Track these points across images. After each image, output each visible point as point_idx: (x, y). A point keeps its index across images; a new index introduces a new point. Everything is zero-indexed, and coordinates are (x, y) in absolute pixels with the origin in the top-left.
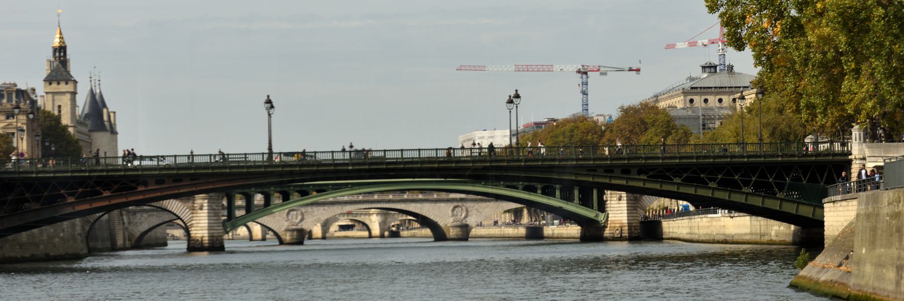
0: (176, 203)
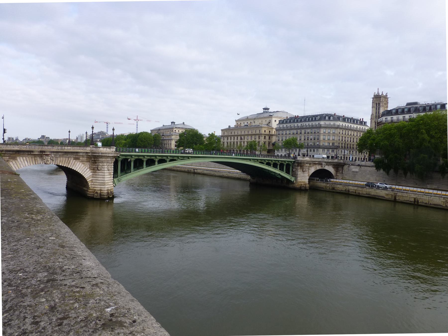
0: (79, 164)
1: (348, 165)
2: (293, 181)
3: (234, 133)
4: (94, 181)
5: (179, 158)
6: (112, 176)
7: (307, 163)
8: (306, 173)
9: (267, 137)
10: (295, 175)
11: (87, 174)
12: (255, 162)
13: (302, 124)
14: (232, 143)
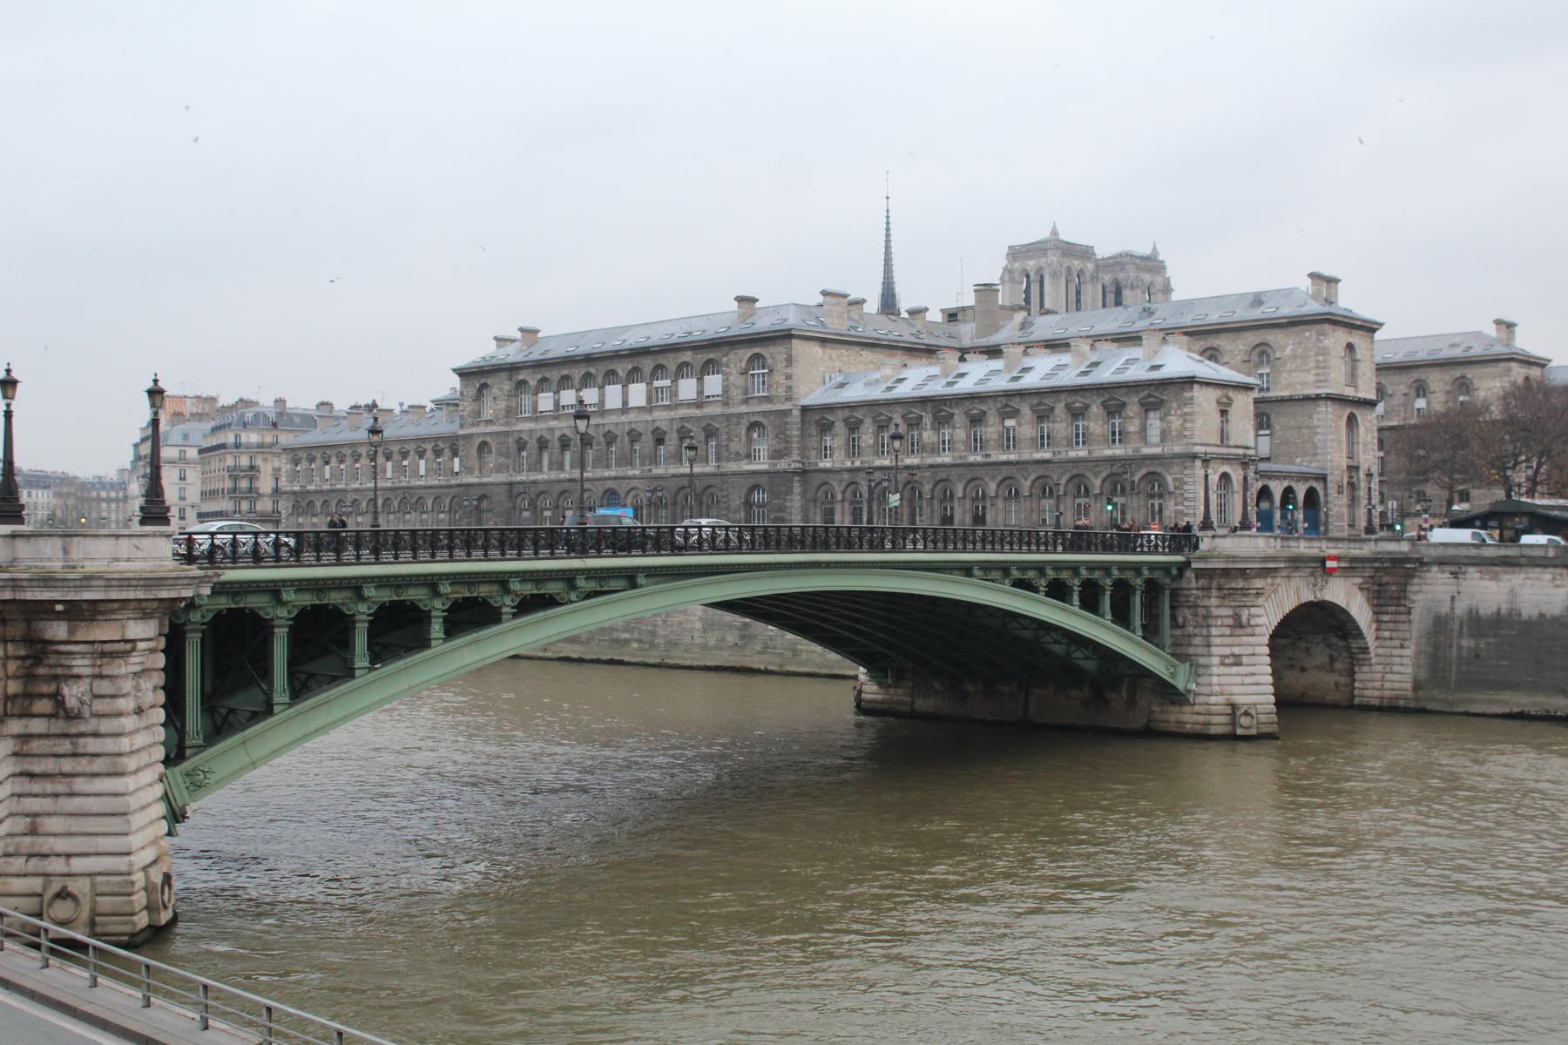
2: (1180, 686)
12: (993, 581)
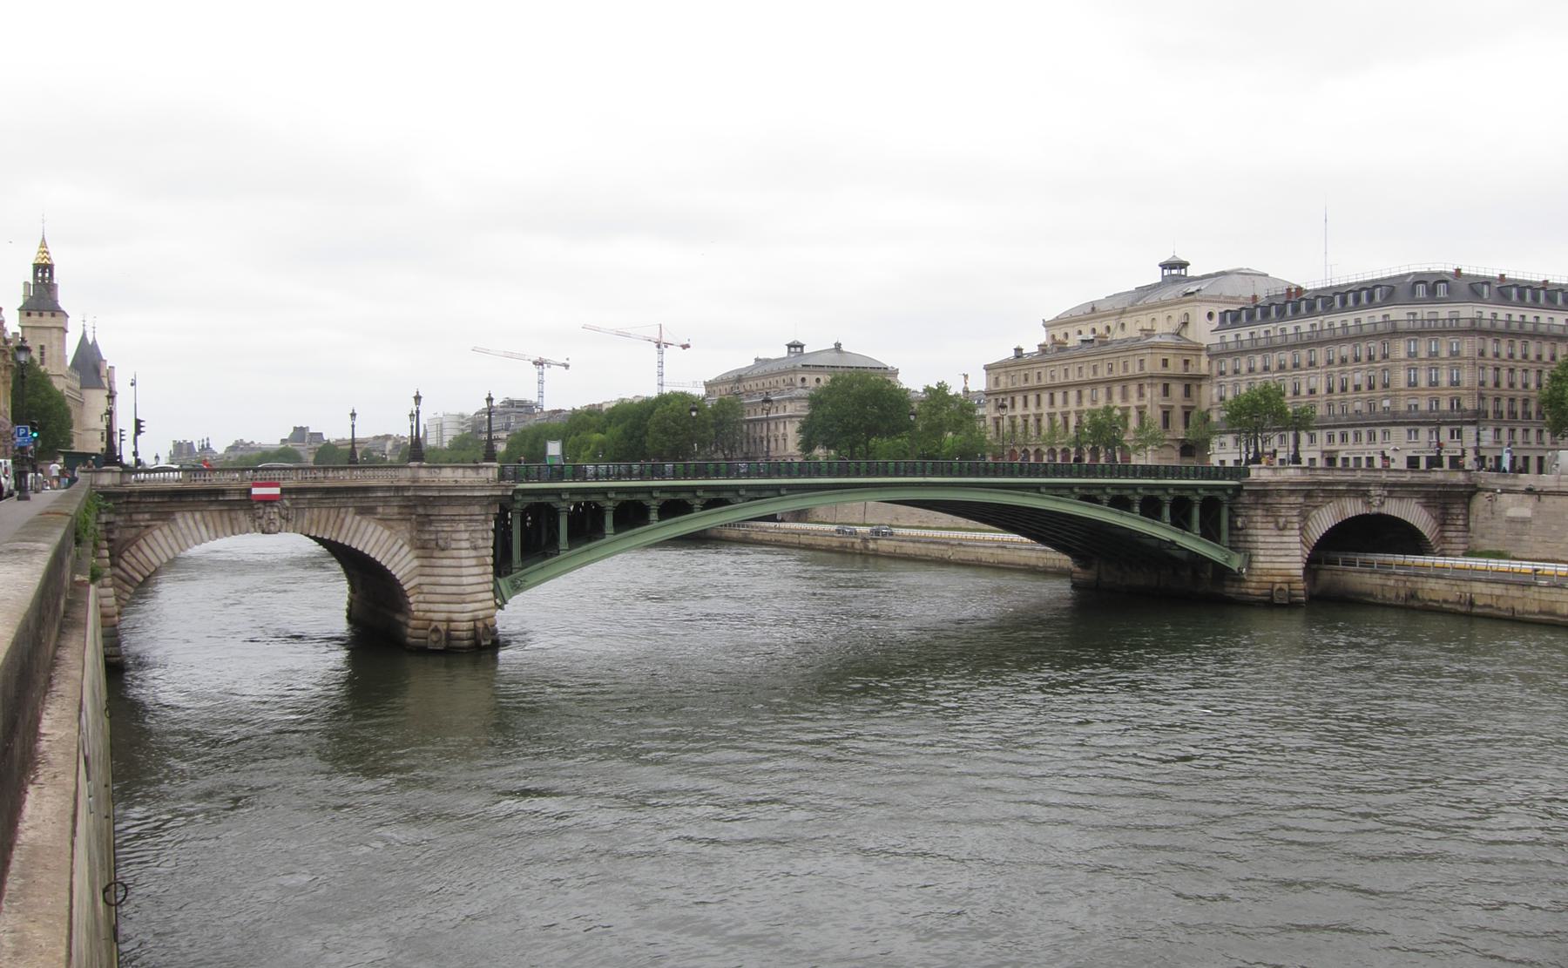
1: (1488, 494)
3: (1039, 378)
4: (426, 589)
5: (742, 492)
6: (491, 569)
7: (1292, 492)
8: (1293, 532)
9: (1177, 390)
10: (1241, 540)
11: (404, 563)
13: (1315, 324)
14: (1032, 420)
